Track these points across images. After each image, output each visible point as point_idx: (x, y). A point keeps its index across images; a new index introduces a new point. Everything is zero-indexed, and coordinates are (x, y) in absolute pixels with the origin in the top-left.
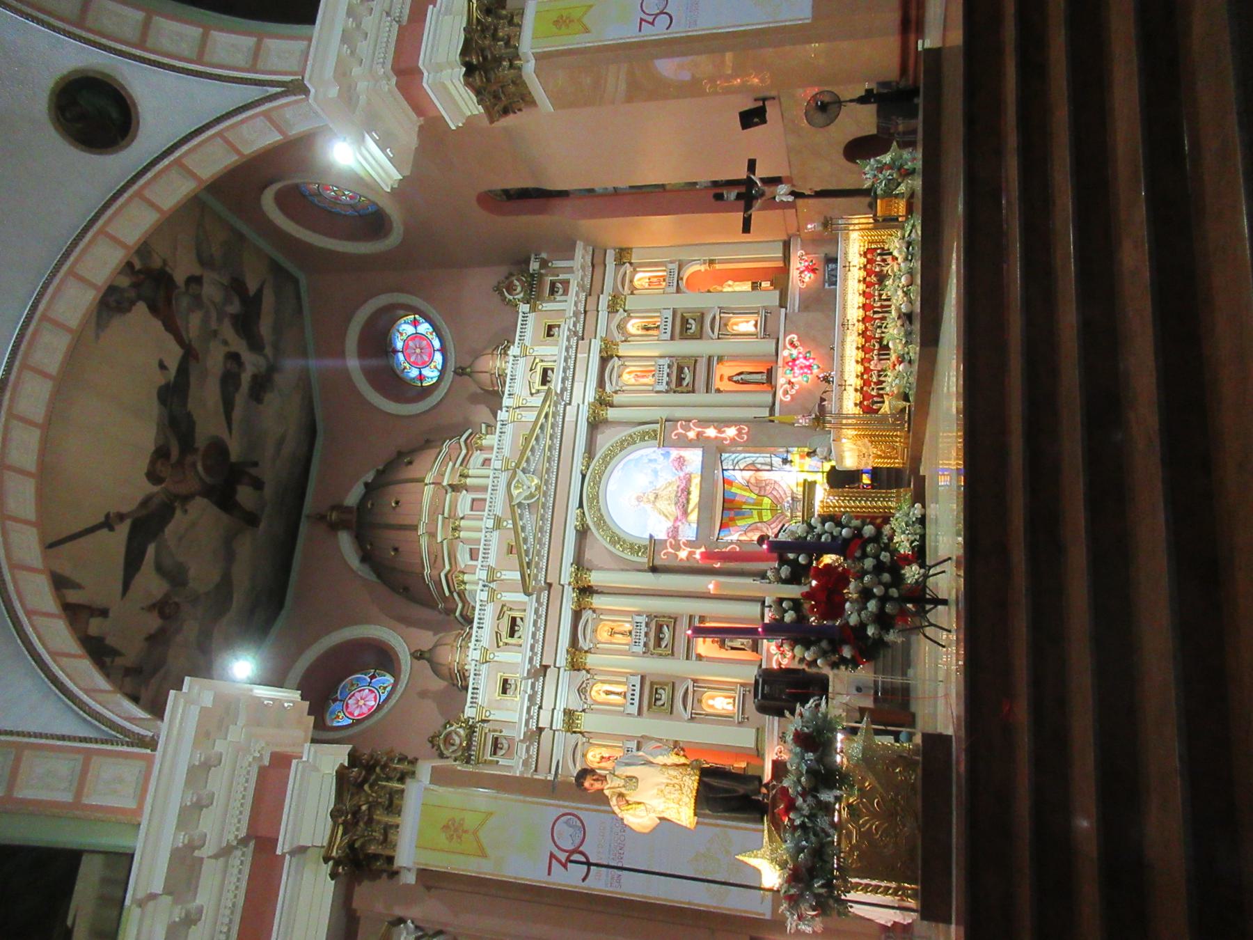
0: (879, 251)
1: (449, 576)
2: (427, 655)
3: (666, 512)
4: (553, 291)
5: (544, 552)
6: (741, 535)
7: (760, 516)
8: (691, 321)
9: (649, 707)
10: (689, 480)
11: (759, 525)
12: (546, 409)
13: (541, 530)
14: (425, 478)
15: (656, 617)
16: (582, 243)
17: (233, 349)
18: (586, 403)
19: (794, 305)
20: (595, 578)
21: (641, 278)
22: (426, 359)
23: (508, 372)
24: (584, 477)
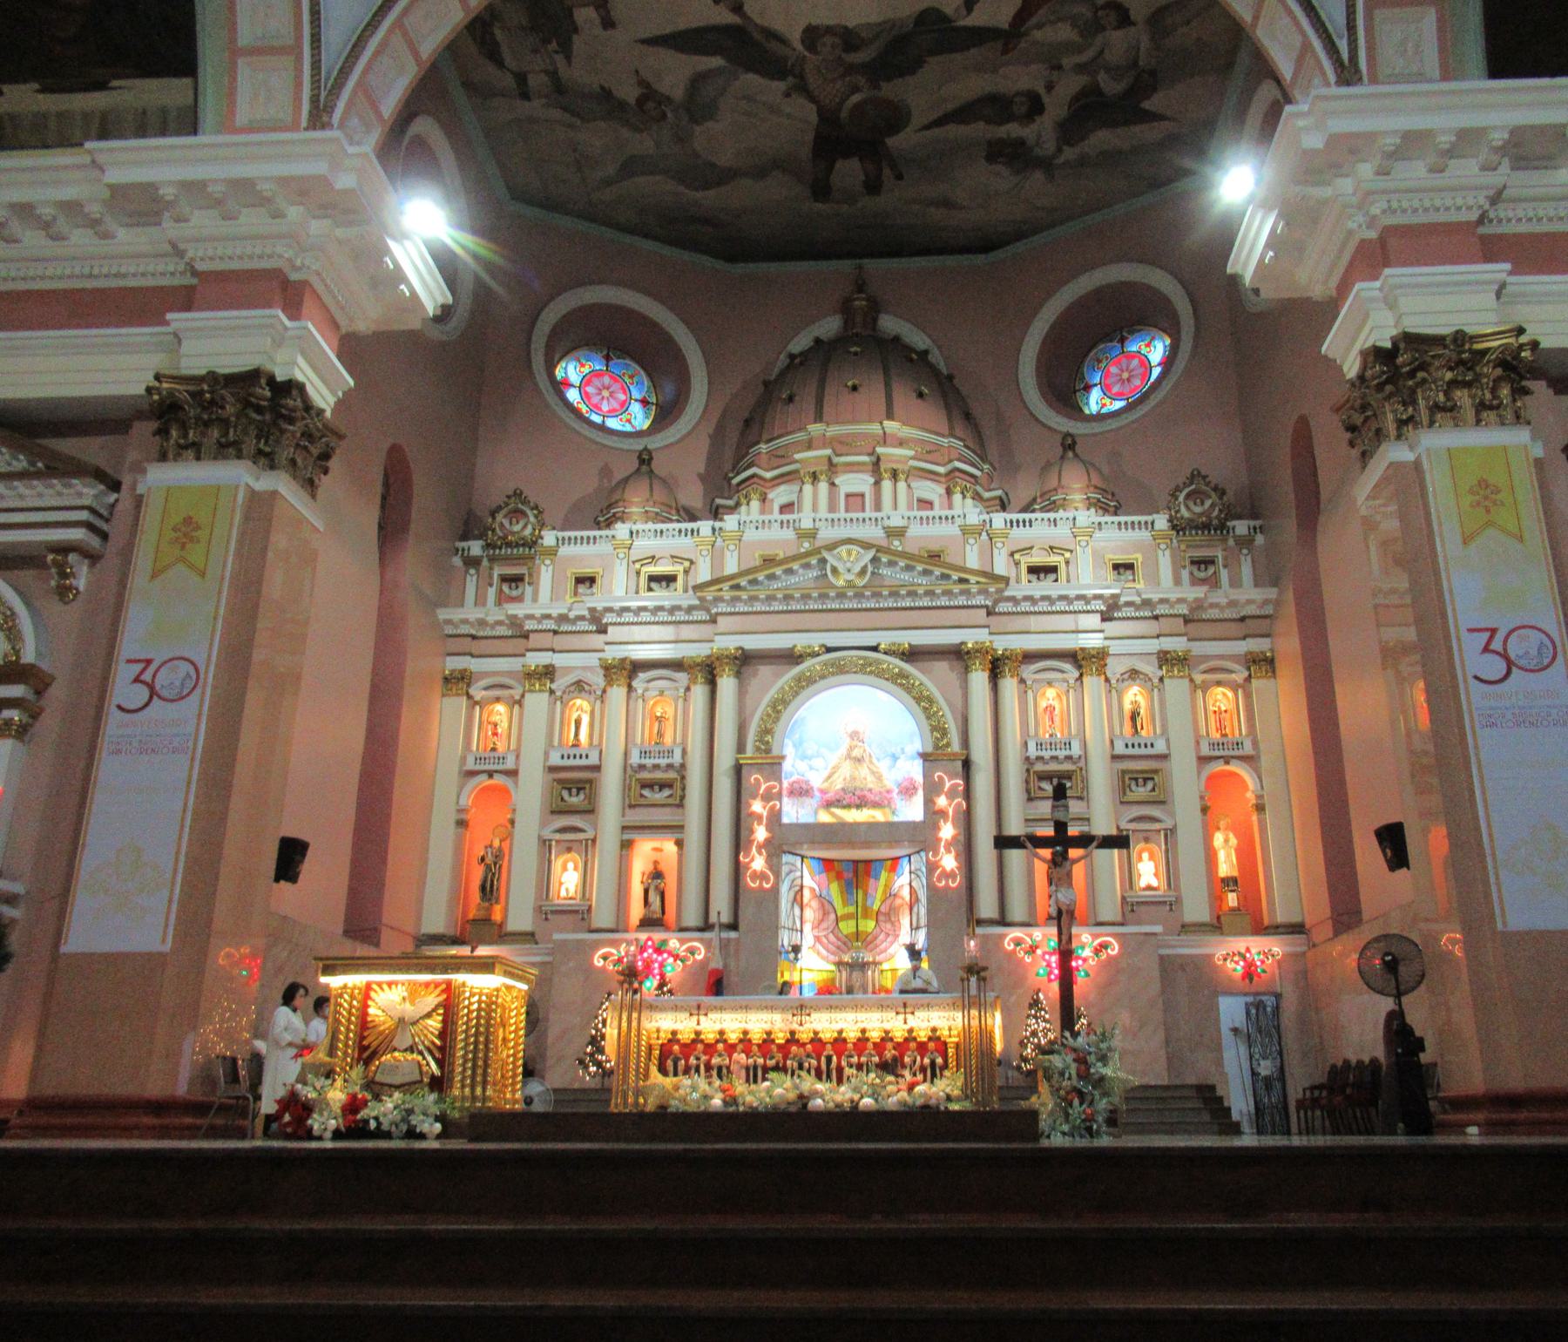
0: (939, 1060)
1: (755, 480)
2: (644, 468)
3: (836, 775)
4: (1203, 563)
5: (758, 607)
6: (812, 890)
7: (847, 917)
9: (560, 781)
10: (876, 805)
11: (832, 916)
12: (973, 579)
13: (788, 598)
14: (893, 420)
15: (683, 778)
16: (1274, 596)
17: (1046, 99)
18: (1107, 643)
19: (1183, 946)
21: (1221, 698)
22: (1116, 389)
23: (1061, 514)
24: (875, 649)
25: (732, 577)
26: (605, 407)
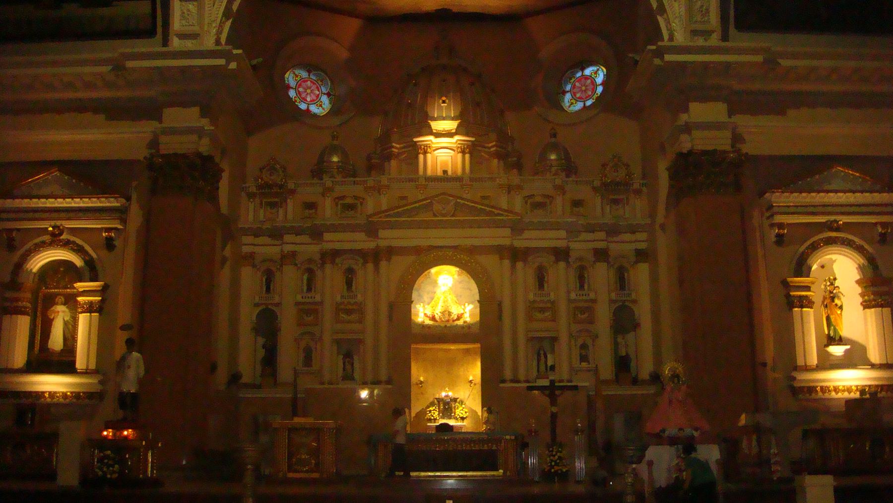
8: (586, 315)
20: (383, 264)
22: (578, 95)
25: (386, 211)
26: (309, 99)
